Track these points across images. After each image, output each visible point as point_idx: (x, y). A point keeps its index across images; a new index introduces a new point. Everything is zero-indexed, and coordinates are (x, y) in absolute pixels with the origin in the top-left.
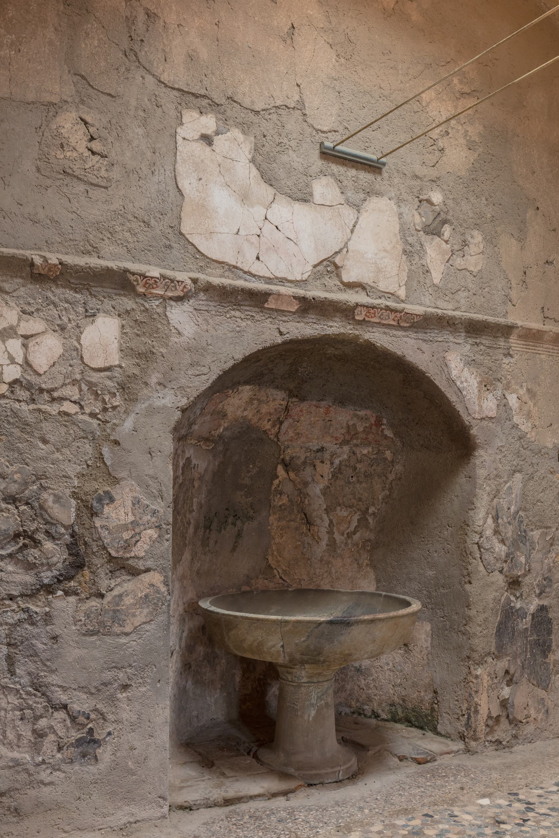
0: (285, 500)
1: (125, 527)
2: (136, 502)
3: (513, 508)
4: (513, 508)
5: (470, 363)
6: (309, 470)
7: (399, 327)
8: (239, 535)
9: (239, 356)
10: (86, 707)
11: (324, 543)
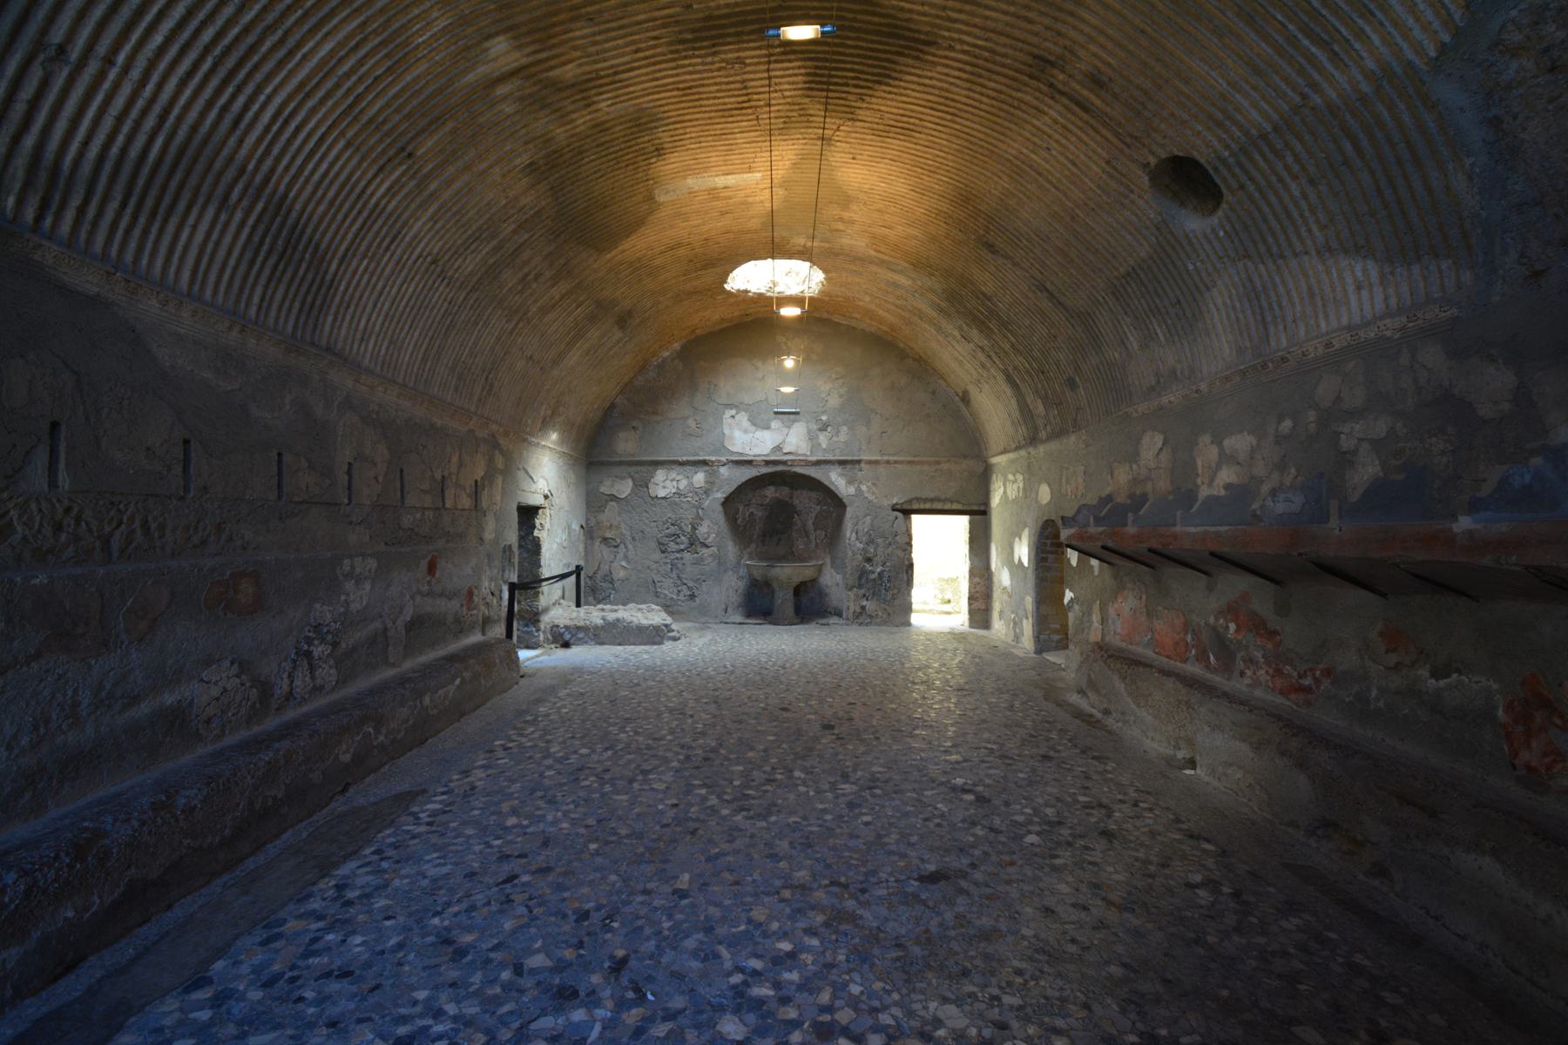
5: (841, 475)
8: (780, 539)
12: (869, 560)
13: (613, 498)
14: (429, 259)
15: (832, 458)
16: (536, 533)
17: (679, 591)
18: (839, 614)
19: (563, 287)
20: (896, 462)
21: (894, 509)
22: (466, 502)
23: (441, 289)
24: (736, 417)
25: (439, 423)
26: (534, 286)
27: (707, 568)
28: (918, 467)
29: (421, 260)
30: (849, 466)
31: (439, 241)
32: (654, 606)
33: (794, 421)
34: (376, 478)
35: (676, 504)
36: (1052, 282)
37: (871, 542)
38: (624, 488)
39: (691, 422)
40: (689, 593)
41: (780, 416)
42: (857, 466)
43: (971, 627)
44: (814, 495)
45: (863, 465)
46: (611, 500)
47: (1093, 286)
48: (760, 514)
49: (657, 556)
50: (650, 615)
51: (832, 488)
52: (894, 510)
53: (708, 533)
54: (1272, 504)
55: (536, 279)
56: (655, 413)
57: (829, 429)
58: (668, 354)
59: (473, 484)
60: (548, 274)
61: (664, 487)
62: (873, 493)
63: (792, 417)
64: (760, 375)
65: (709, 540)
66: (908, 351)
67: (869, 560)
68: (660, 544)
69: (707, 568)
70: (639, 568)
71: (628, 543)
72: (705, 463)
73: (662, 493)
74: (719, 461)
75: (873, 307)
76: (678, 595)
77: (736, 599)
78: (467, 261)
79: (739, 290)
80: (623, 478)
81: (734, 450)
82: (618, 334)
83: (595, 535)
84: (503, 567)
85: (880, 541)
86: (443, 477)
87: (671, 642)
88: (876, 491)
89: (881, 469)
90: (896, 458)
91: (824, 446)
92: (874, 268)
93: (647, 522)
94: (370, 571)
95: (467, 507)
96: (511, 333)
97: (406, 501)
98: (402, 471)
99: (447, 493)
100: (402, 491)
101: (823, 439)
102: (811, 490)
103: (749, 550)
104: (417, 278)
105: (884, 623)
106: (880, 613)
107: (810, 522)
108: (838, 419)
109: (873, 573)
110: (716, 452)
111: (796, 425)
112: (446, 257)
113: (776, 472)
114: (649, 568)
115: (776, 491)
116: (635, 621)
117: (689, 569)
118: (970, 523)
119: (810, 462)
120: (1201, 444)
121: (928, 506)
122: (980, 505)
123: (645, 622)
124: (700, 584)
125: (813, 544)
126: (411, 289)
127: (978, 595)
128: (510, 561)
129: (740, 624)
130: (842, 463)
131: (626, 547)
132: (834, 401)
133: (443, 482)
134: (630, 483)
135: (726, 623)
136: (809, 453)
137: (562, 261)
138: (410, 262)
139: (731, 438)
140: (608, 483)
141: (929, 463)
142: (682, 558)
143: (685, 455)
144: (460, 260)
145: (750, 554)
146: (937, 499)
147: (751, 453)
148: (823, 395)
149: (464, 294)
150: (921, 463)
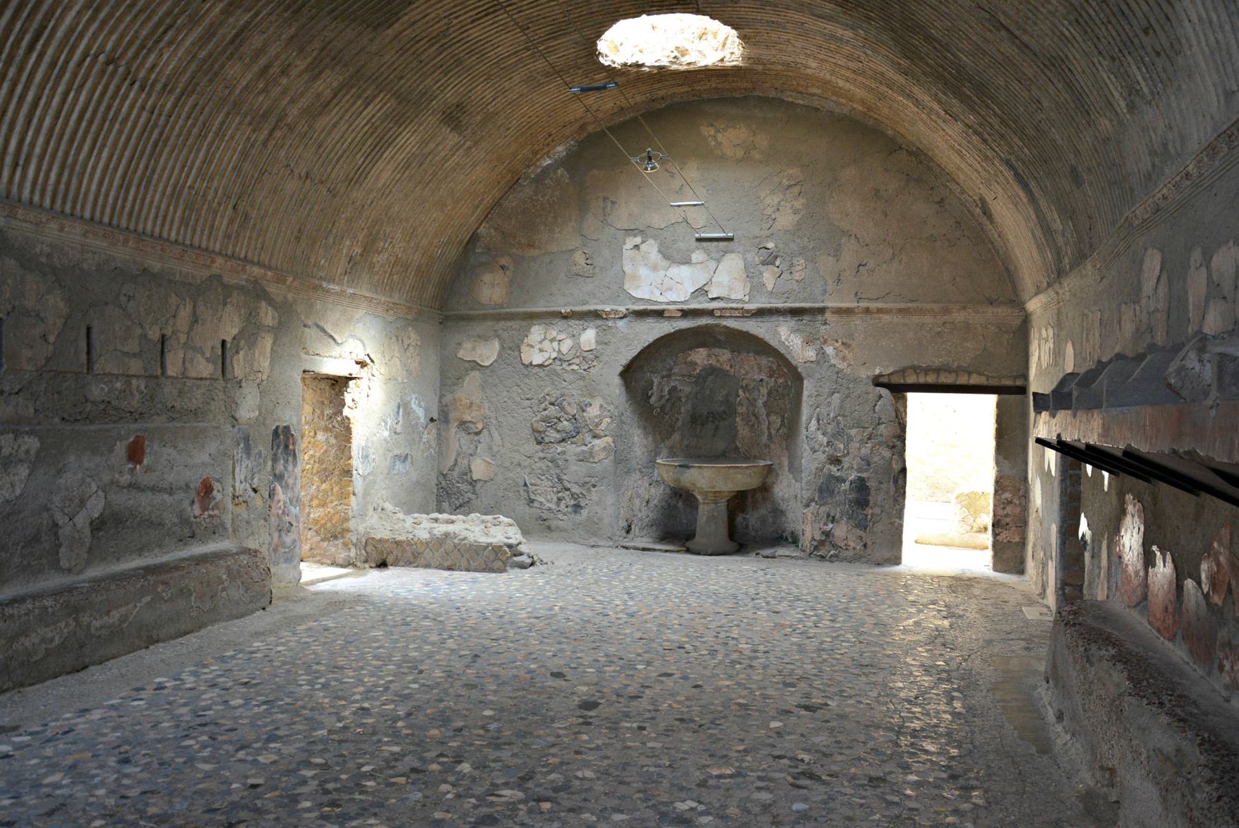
0: (744, 409)
1: (596, 417)
2: (601, 406)
3: (832, 415)
4: (832, 415)
5: (794, 331)
6: (756, 393)
7: (743, 317)
8: (717, 428)
9: (651, 340)
10: (577, 491)
11: (766, 434)
12: (836, 461)
13: (476, 366)
14: (102, 58)
15: (780, 305)
16: (346, 412)
17: (560, 500)
18: (794, 541)
19: (329, 81)
20: (880, 311)
21: (877, 382)
22: (204, 368)
23: (132, 95)
24: (643, 247)
25: (156, 266)
26: (284, 81)
27: (598, 467)
28: (915, 319)
29: (88, 60)
30: (806, 318)
31: (110, 33)
32: (502, 518)
33: (726, 252)
34: (44, 337)
35: (557, 374)
36: (1004, 13)
37: (839, 434)
38: (488, 353)
39: (579, 258)
40: (573, 502)
41: (705, 244)
42: (819, 317)
43: (996, 569)
44: (764, 361)
45: (828, 315)
46: (473, 369)
47: (1051, 13)
48: (687, 389)
49: (532, 447)
50: (493, 530)
51: (783, 351)
52: (877, 384)
53: (601, 418)
54: (1197, 366)
55: (285, 72)
56: (531, 245)
57: (777, 263)
58: (549, 162)
59: (219, 346)
60: (302, 64)
61: (541, 350)
62: (844, 359)
63: (722, 244)
64: (677, 183)
65: (603, 426)
66: (900, 140)
67: (836, 461)
68: (535, 431)
69: (598, 467)
70: (507, 464)
71: (493, 429)
72: (596, 315)
73: (538, 359)
74: (616, 312)
75: (828, 76)
76: (558, 504)
77: (644, 514)
78: (165, 57)
79: (625, 65)
80: (484, 338)
81: (637, 294)
82: (453, 138)
83: (452, 416)
84: (275, 455)
85: (853, 432)
86: (163, 336)
87: (517, 570)
88: (850, 356)
89: (857, 322)
90: (880, 305)
91: (770, 287)
92: (797, 17)
93: (518, 399)
94: (27, 452)
95: (206, 374)
96: (265, 144)
97: (96, 367)
98: (89, 329)
99: (169, 357)
100: (89, 353)
101: (769, 277)
102: (757, 353)
103: (667, 443)
104: (89, 84)
105: (856, 559)
106: (852, 544)
107: (760, 403)
108: (792, 246)
109: (844, 481)
110: (614, 298)
111: (730, 256)
112: (130, 54)
113: (699, 327)
114: (519, 465)
115: (709, 356)
116: (471, 537)
117: (573, 468)
118: (999, 405)
119: (748, 311)
120: (1193, 268)
121: (931, 379)
122: (1015, 378)
123: (484, 540)
124: (589, 491)
125: (765, 438)
126: (82, 99)
127: (1008, 520)
128: (286, 447)
129: (644, 549)
130: (795, 313)
131: (490, 434)
132: (786, 220)
133: (163, 344)
134: (496, 345)
135: (627, 548)
136: (747, 297)
137: (317, 44)
138: (72, 65)
139: (635, 277)
140: (468, 345)
141: (933, 313)
142: (564, 453)
143: (569, 304)
144: (152, 57)
145: (671, 448)
146: (947, 369)
147: (661, 299)
148: (769, 211)
149: (172, 99)
150: (921, 312)
